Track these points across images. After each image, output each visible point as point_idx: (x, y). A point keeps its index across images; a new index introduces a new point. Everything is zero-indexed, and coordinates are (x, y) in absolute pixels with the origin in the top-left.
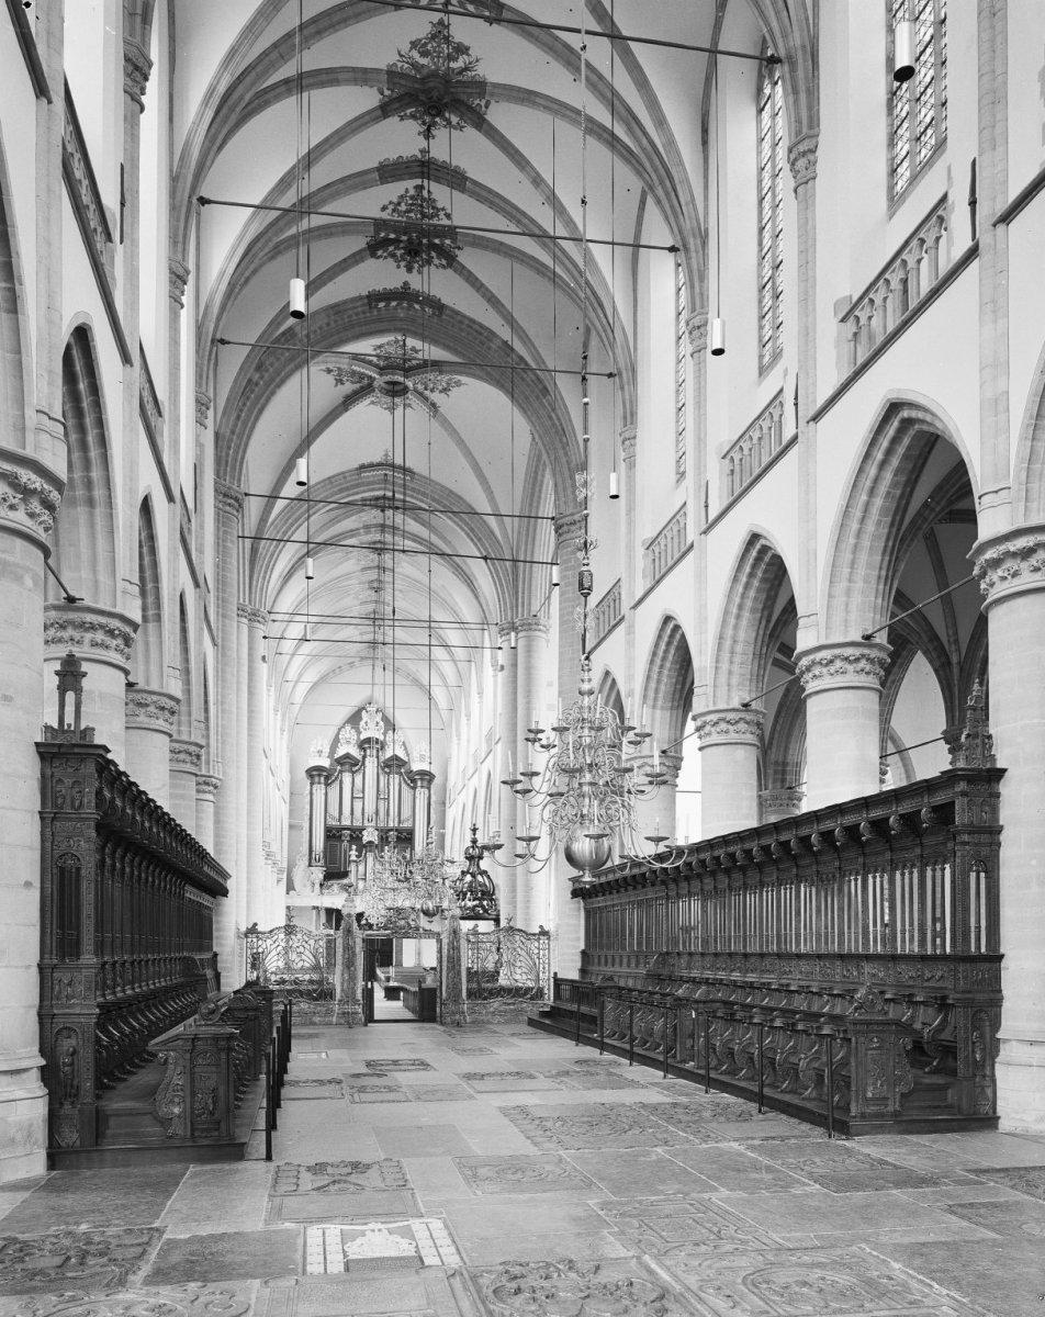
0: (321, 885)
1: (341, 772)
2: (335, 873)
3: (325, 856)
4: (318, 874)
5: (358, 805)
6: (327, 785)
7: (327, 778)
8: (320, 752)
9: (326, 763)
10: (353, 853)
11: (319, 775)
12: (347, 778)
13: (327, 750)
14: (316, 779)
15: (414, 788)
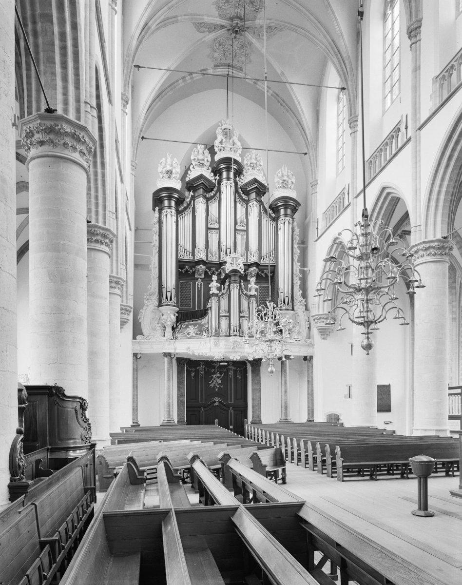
0: (173, 329)
1: (193, 198)
2: (190, 313)
3: (177, 295)
4: (170, 314)
5: (213, 237)
6: (179, 213)
7: (179, 202)
8: (169, 173)
9: (178, 185)
10: (214, 285)
11: (170, 198)
12: (200, 205)
13: (178, 171)
14: (166, 203)
15: (276, 219)
